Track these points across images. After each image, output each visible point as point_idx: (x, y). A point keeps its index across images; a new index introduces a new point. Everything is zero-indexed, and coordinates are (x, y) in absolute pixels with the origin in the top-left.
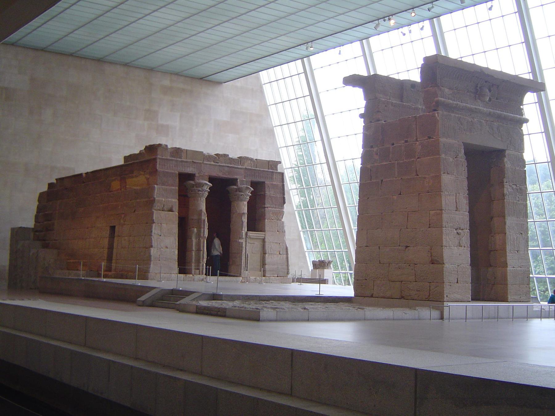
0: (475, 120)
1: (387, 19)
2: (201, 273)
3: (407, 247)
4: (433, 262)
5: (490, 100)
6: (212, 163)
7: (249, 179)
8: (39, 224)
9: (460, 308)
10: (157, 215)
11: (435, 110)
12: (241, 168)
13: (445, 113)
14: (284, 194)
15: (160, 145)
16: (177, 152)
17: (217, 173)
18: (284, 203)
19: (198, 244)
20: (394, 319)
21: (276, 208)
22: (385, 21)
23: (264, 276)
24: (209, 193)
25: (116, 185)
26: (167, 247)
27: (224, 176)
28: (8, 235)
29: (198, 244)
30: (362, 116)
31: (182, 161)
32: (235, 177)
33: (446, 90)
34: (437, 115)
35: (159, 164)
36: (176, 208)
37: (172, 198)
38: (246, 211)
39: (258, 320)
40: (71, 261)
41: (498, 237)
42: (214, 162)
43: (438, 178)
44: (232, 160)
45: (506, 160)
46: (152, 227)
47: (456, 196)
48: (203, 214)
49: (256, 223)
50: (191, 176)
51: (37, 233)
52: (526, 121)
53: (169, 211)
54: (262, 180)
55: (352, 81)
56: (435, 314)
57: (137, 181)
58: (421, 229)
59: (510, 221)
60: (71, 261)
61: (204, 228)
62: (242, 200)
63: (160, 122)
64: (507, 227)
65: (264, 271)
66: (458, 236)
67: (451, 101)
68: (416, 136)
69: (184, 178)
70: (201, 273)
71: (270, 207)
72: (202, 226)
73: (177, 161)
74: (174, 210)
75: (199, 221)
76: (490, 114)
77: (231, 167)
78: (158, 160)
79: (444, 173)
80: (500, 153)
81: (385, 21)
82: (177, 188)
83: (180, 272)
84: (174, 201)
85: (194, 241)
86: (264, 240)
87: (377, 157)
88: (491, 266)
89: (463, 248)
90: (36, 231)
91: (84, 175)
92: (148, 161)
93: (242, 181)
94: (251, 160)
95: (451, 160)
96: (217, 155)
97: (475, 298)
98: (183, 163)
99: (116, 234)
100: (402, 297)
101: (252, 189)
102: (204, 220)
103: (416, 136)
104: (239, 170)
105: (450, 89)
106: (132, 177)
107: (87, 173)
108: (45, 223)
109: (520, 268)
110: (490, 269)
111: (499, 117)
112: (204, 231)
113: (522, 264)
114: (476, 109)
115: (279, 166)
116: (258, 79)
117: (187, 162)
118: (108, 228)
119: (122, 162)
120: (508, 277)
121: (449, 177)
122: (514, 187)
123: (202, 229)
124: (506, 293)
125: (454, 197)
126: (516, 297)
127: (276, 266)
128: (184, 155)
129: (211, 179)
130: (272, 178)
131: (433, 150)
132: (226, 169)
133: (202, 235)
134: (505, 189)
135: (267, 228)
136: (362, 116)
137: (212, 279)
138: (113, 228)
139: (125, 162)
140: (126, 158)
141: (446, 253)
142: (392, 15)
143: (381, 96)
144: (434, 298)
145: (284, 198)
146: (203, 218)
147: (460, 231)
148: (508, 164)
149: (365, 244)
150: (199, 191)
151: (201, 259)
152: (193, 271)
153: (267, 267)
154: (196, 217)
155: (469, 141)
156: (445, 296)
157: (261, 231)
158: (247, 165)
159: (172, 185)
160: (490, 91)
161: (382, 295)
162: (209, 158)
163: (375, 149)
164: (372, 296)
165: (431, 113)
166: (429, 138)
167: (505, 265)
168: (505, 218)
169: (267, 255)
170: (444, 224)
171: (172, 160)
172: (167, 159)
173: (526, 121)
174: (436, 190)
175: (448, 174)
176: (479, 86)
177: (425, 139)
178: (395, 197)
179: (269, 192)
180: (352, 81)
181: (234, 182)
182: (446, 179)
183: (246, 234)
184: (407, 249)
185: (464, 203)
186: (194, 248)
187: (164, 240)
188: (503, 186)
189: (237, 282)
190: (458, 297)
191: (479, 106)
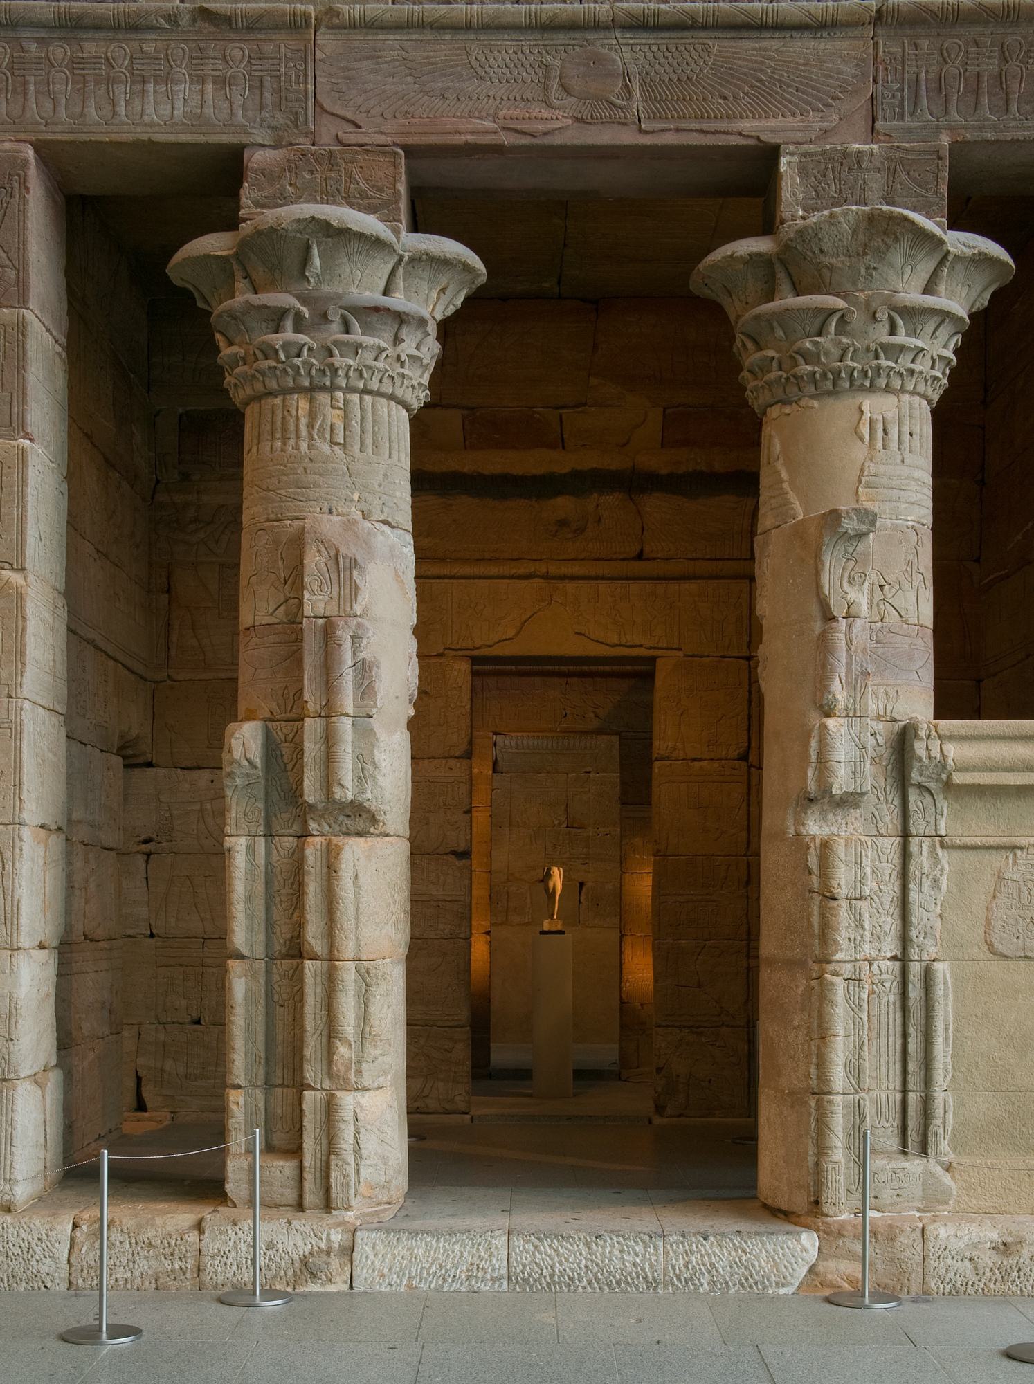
32: (751, 127)
62: (833, 384)
75: (306, 652)
85: (245, 854)
93: (835, 171)
98: (91, 48)
112: (329, 739)
123: (312, 727)
132: (627, 54)
133: (311, 793)
150: (277, 318)
151: (312, 1046)
152: (235, 1169)
183: (902, 742)
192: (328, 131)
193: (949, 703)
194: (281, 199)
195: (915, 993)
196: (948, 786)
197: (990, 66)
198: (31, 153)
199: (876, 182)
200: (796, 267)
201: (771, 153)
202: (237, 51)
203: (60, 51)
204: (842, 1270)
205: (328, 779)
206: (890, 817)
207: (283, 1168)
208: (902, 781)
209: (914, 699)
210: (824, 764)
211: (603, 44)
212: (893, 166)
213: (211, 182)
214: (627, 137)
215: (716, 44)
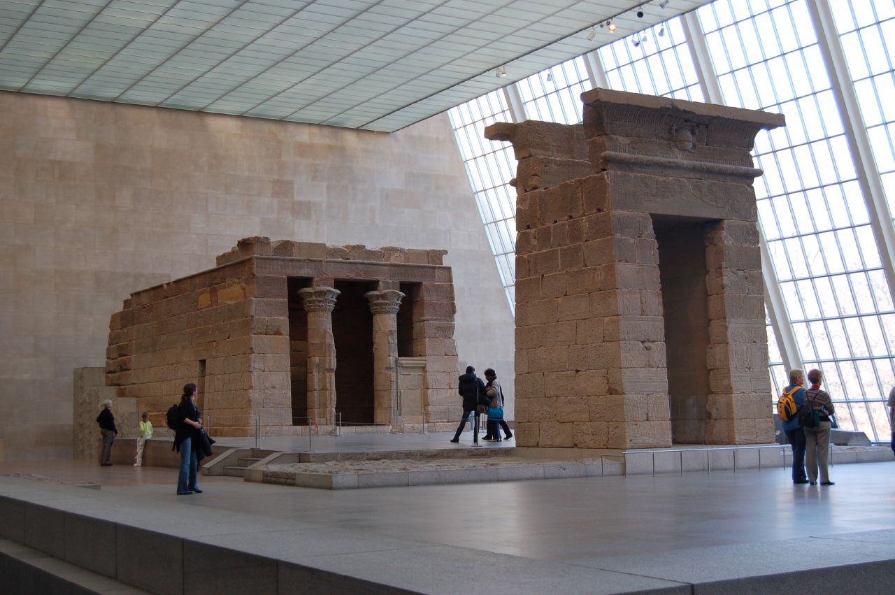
0: (671, 179)
1: (605, 23)
2: (328, 422)
3: (577, 371)
4: (611, 391)
5: (694, 146)
6: (340, 260)
7: (398, 280)
8: (111, 361)
9: (656, 458)
10: (257, 340)
11: (604, 170)
12: (384, 265)
13: (619, 172)
14: (453, 298)
15: (257, 239)
16: (286, 246)
17: (345, 274)
18: (454, 311)
19: (323, 380)
20: (545, 478)
22: (602, 26)
23: (428, 422)
24: (336, 304)
25: (204, 300)
26: (274, 388)
27: (358, 278)
28: (69, 379)
29: (323, 380)
30: (513, 183)
31: (292, 260)
33: (621, 139)
34: (606, 176)
35: (257, 266)
36: (286, 329)
37: (279, 315)
38: (395, 328)
39: (331, 488)
40: (154, 413)
41: (718, 350)
42: (342, 258)
43: (610, 269)
44: (371, 254)
45: (724, 233)
46: (249, 359)
47: (641, 294)
48: (327, 335)
50: (307, 281)
51: (110, 375)
52: (759, 173)
53: (275, 334)
54: (418, 280)
55: (498, 132)
56: (612, 467)
57: (231, 293)
58: (594, 345)
59: (735, 326)
60: (154, 413)
61: (330, 356)
63: (297, 198)
64: (729, 334)
65: (427, 414)
66: (645, 352)
67: (626, 155)
68: (583, 209)
69: (297, 286)
70: (328, 422)
71: (431, 320)
72: (327, 354)
73: (283, 260)
76: (694, 169)
77: (369, 264)
78: (255, 262)
79: (620, 261)
80: (715, 224)
81: (602, 26)
82: (286, 300)
83: (296, 423)
84: (283, 320)
86: (424, 368)
87: (534, 242)
88: (712, 393)
89: (655, 369)
90: (109, 373)
91: (165, 286)
92: (242, 263)
93: (387, 285)
94: (401, 251)
95: (632, 241)
96: (347, 247)
97: (676, 442)
98: (294, 263)
99: (207, 371)
100: (576, 445)
101: (402, 294)
102: (330, 345)
103: (583, 209)
105: (627, 136)
106: (224, 287)
107: (168, 284)
108: (120, 359)
109: (753, 394)
110: (711, 397)
111: (710, 172)
112: (330, 360)
114: (669, 162)
115: (445, 257)
116: (447, 122)
117: (299, 261)
118: (198, 364)
119: (213, 266)
120: (735, 408)
121: (629, 265)
124: (731, 430)
125: (638, 295)
126: (749, 437)
127: (444, 407)
128: (295, 250)
129: (338, 283)
130: (434, 276)
131: (603, 229)
132: (361, 267)
134: (726, 281)
135: (428, 352)
136: (513, 183)
137: (346, 431)
138: (203, 362)
139: (218, 264)
140: (219, 259)
141: (627, 378)
142: (611, 18)
143: (539, 151)
144: (613, 444)
145: (453, 306)
146: (327, 341)
147: (650, 344)
148: (727, 239)
149: (526, 371)
154: (317, 341)
155: (660, 212)
156: (628, 441)
157: (420, 355)
158: (393, 261)
159: (278, 296)
160: (693, 133)
161: (549, 443)
162: (335, 252)
163: (533, 231)
164: (537, 446)
165: (599, 175)
166: (599, 210)
167: (729, 390)
168: (725, 322)
170: (622, 336)
171: (277, 259)
172: (269, 259)
173: (759, 173)
174: (608, 289)
175: (627, 261)
176: (674, 128)
177: (593, 212)
178: (560, 300)
179: (427, 297)
180: (498, 132)
181: (373, 285)
182: (625, 270)
183: (396, 361)
184: (578, 375)
185: (655, 302)
186: (316, 387)
187: (270, 375)
188: (721, 275)
189: (385, 433)
190: (650, 440)
191: (677, 157)
192: (324, 275)
193: (400, 355)
195: (399, 394)
196: (403, 367)
197: (403, 271)
198: (286, 277)
201: (378, 281)
202: (313, 264)
204: (394, 430)
205: (330, 366)
207: (325, 419)
208: (397, 366)
209: (396, 355)
210: (390, 364)
212: (393, 283)
214: (361, 278)
215: (372, 267)
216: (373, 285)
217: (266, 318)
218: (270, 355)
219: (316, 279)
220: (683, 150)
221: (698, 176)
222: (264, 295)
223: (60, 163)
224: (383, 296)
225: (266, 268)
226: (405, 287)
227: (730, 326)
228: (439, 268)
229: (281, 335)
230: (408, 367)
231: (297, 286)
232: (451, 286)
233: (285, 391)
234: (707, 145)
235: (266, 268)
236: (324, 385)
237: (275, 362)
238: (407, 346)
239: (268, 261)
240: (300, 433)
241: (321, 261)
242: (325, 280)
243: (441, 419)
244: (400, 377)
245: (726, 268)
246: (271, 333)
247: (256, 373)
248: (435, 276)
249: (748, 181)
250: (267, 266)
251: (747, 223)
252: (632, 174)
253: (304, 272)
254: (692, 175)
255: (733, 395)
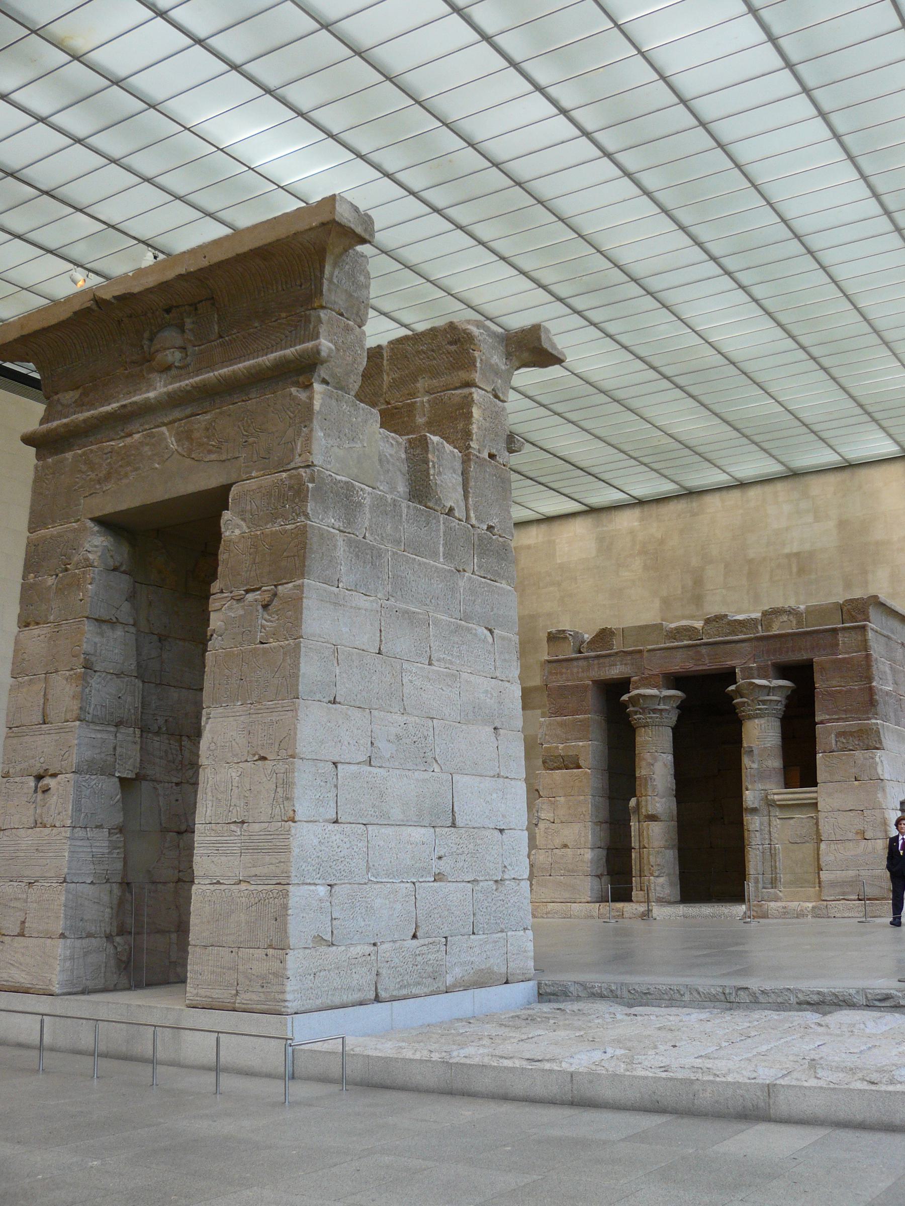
13: (50, 460)
16: (604, 636)
17: (680, 664)
21: (846, 720)
49: (800, 766)
66: (40, 795)
71: (829, 721)
74: (581, 763)
76: (175, 401)
94: (790, 612)
98: (601, 660)
104: (739, 645)
113: (254, 871)
114: (124, 406)
122: (250, 597)
127: (852, 873)
135: (821, 776)
153: (824, 875)
169: (823, 846)
175: (37, 624)
181: (729, 676)
194: (637, 688)
199: (755, 673)
200: (739, 693)
201: (734, 668)
202: (629, 658)
203: (596, 662)
206: (765, 813)
211: (699, 649)
212: (759, 668)
213: (623, 685)
216: (729, 676)
217: (561, 746)
218: (562, 799)
219: (633, 679)
220: (167, 368)
221: (188, 411)
222: (558, 712)
223: (797, 554)
224: (739, 693)
225: (561, 674)
226: (783, 671)
227: (208, 727)
228: (844, 629)
229: (579, 767)
230: (793, 805)
231: (613, 693)
232: (868, 657)
233: (582, 851)
234: (221, 337)
235: (561, 674)
236: (655, 842)
237: (569, 808)
238: (800, 766)
239: (565, 664)
240: (596, 914)
241: (640, 651)
242: (646, 678)
243: (844, 894)
244: (776, 822)
245: (222, 592)
246: (572, 766)
247: (542, 825)
248: (838, 645)
249: (301, 379)
250: (564, 670)
251: (284, 475)
252: (69, 455)
253: (616, 671)
254: (177, 414)
255: (194, 887)
